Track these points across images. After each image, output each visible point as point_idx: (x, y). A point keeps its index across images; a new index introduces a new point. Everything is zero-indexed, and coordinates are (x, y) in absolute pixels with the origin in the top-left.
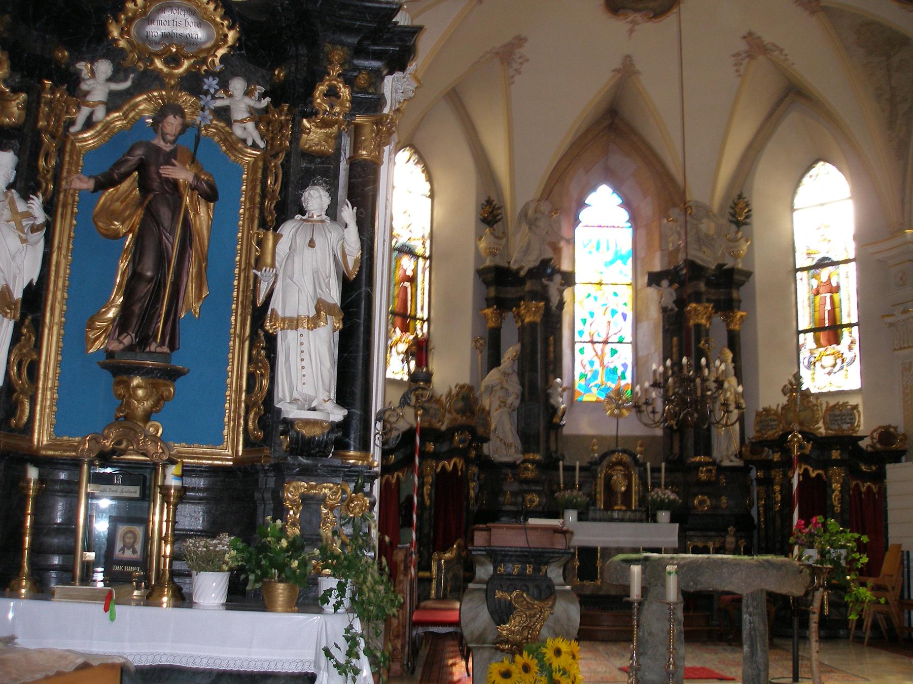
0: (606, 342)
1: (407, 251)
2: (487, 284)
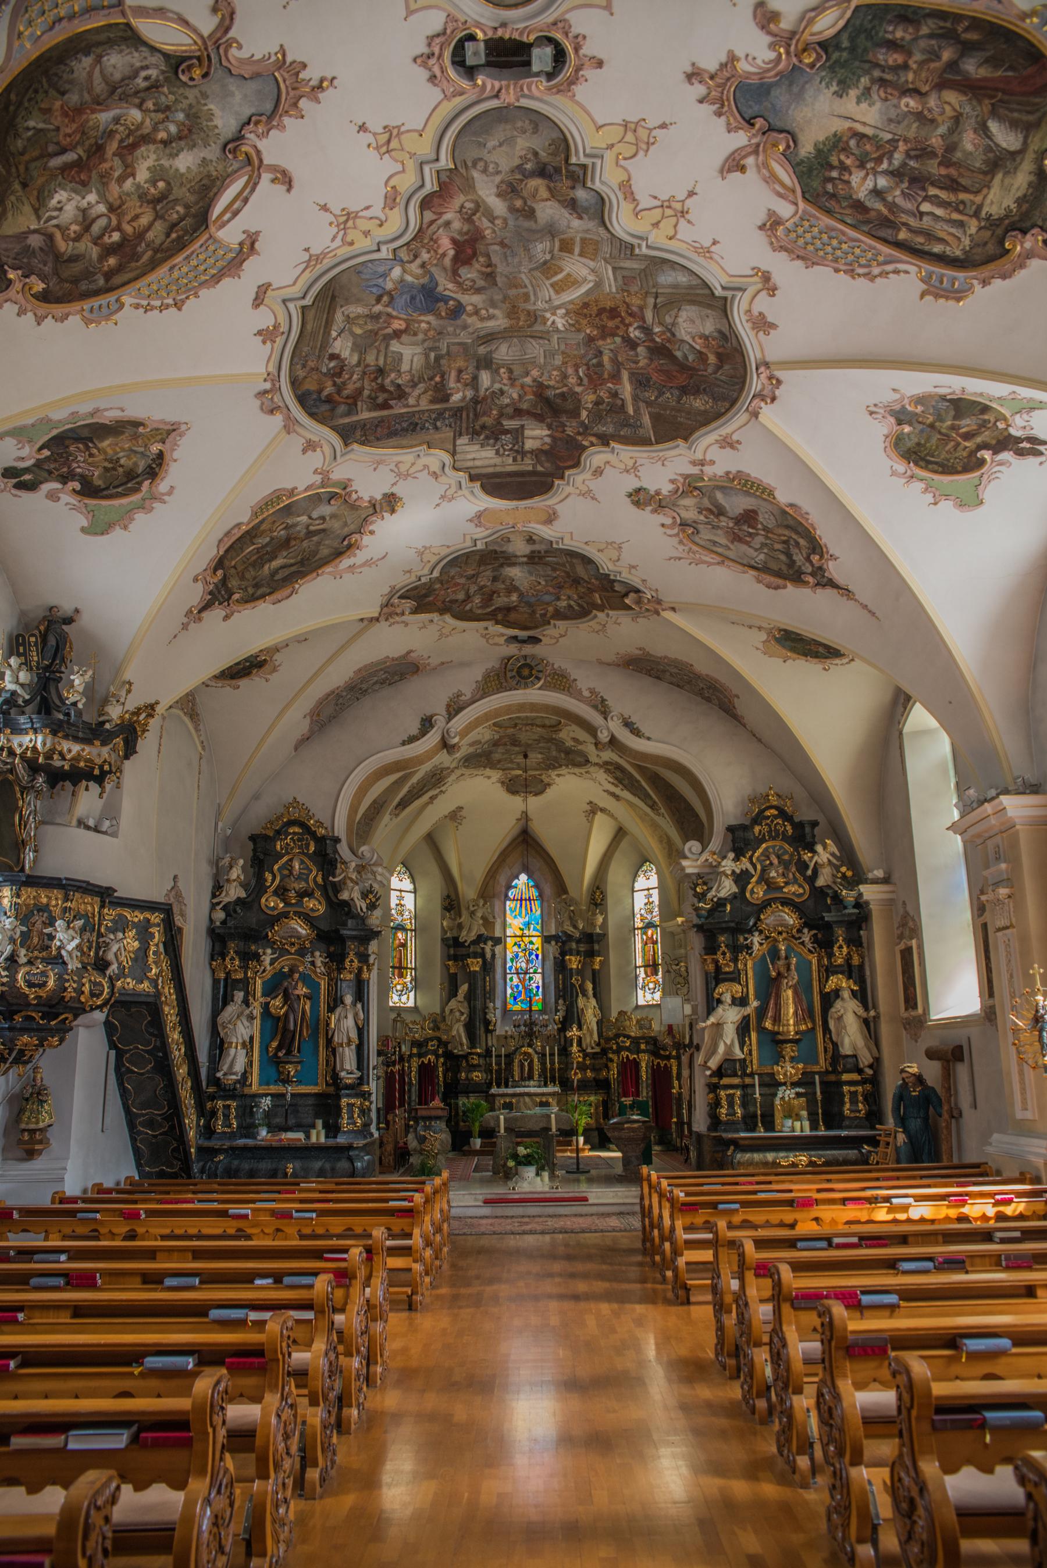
0: (526, 973)
1: (401, 928)
2: (449, 947)
